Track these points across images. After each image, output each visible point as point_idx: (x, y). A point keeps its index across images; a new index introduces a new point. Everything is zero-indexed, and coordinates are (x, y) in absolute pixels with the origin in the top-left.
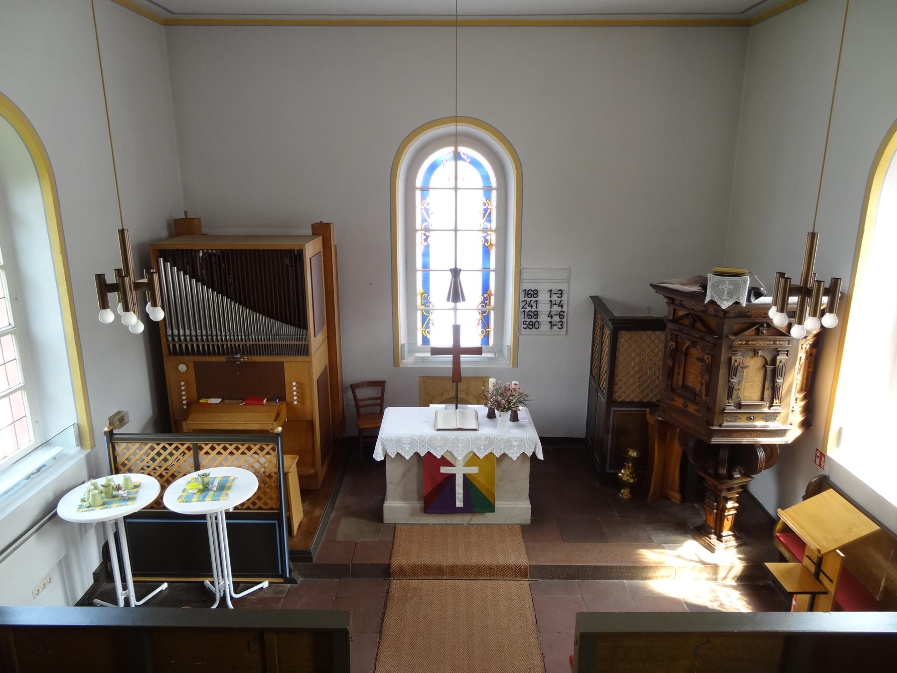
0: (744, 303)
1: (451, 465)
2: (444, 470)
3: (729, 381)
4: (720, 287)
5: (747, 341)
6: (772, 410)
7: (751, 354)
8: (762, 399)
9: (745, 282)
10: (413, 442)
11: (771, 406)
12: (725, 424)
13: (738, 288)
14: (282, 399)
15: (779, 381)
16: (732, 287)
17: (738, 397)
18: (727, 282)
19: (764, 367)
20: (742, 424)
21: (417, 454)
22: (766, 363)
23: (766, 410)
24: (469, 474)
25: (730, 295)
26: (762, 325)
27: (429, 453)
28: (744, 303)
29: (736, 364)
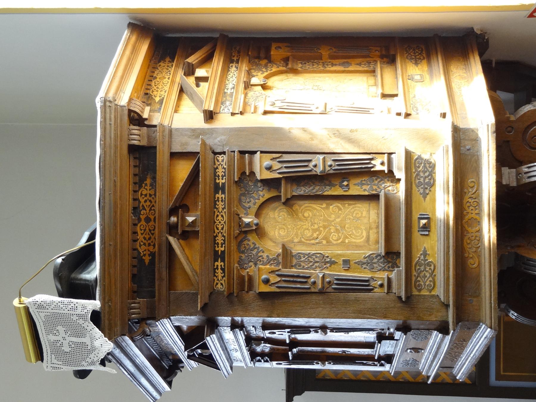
0: (96, 304)
3: (321, 292)
4: (66, 349)
5: (217, 256)
6: (400, 174)
7: (252, 239)
8: (375, 197)
9: (40, 306)
11: (390, 175)
12: (439, 291)
13: (56, 319)
15: (318, 164)
16: (60, 328)
17: (368, 262)
18: (52, 338)
19: (288, 203)
20: (434, 249)
22: (277, 198)
23: (400, 190)
25: (80, 332)
26: (172, 229)
28: (96, 304)
29: (274, 279)
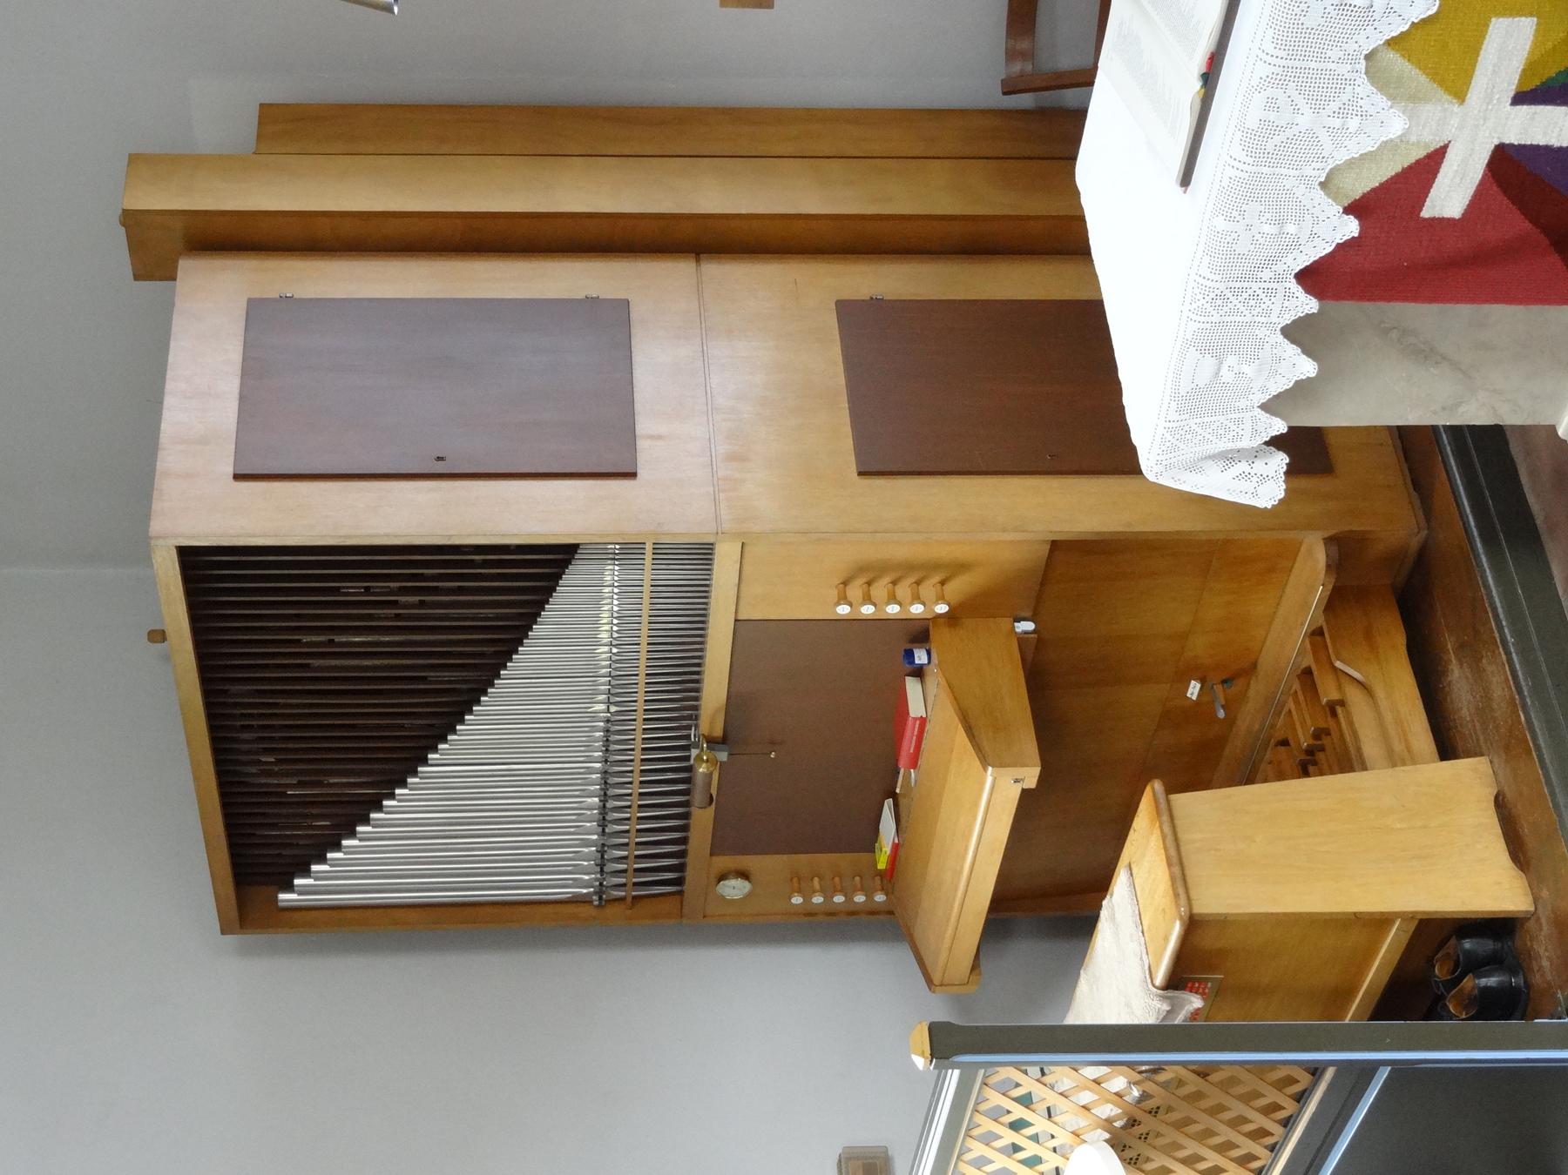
1: (1435, 159)
2: (1450, 197)
10: (1212, 344)
14: (920, 633)
21: (1296, 332)
24: (1527, 72)
27: (1310, 278)
